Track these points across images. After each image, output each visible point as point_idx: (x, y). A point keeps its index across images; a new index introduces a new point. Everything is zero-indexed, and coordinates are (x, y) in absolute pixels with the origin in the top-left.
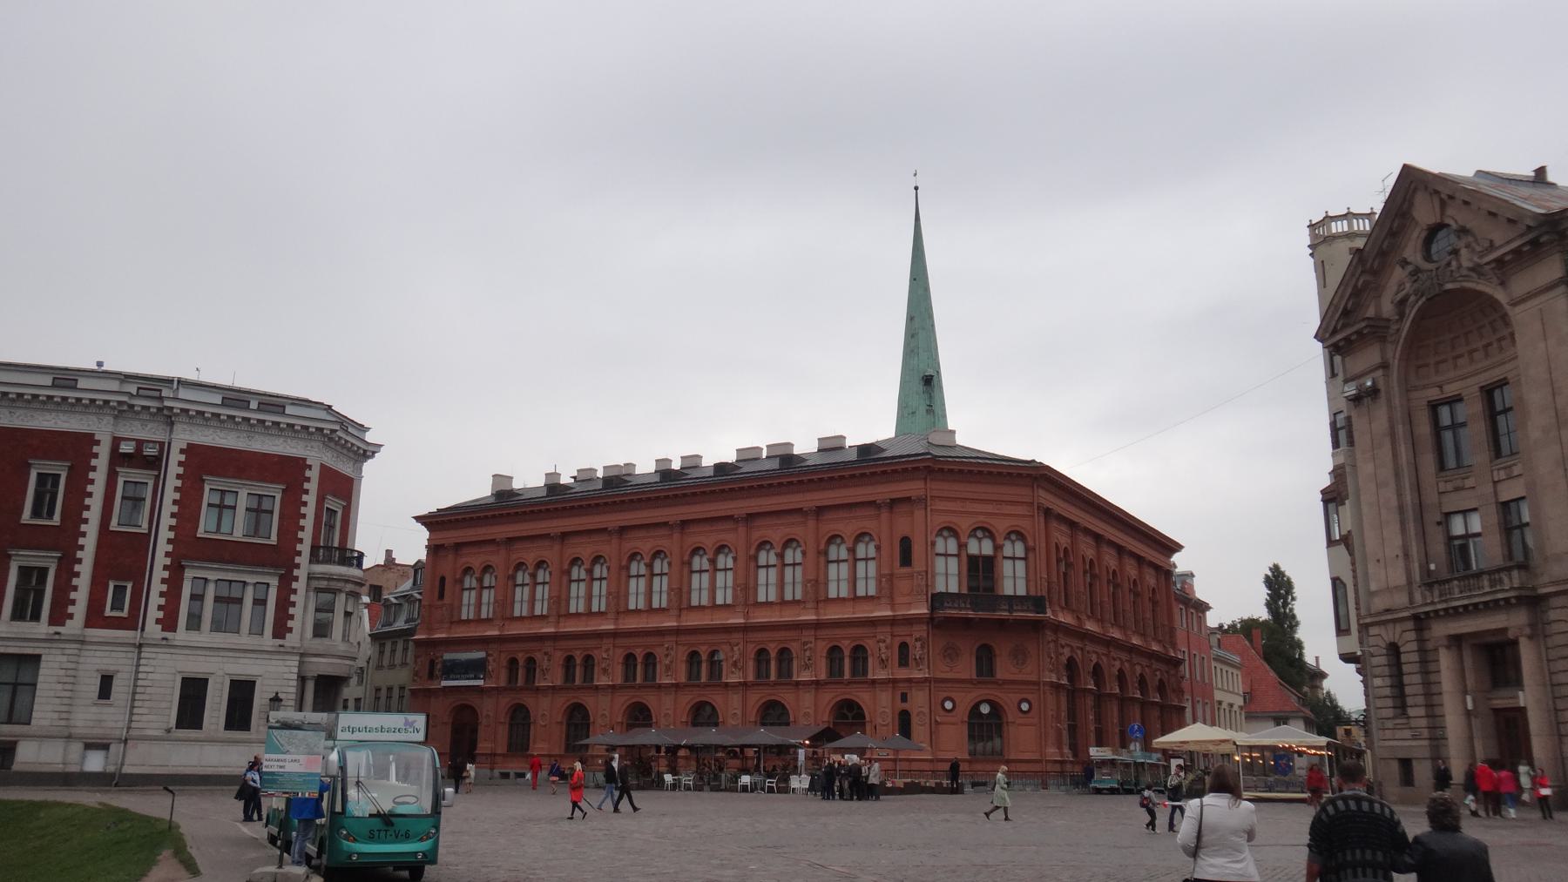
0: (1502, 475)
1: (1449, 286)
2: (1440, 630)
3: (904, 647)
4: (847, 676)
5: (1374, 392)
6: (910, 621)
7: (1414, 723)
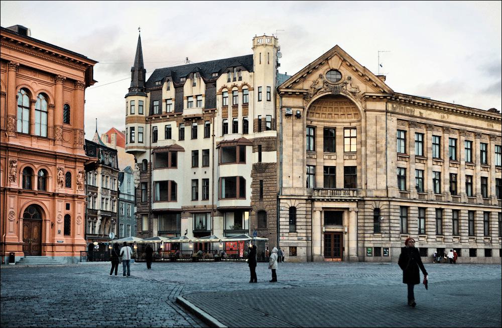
0: (327, 157)
1: (341, 93)
2: (318, 205)
3: (68, 175)
4: (36, 188)
5: (298, 116)
6: (75, 160)
7: (299, 235)
